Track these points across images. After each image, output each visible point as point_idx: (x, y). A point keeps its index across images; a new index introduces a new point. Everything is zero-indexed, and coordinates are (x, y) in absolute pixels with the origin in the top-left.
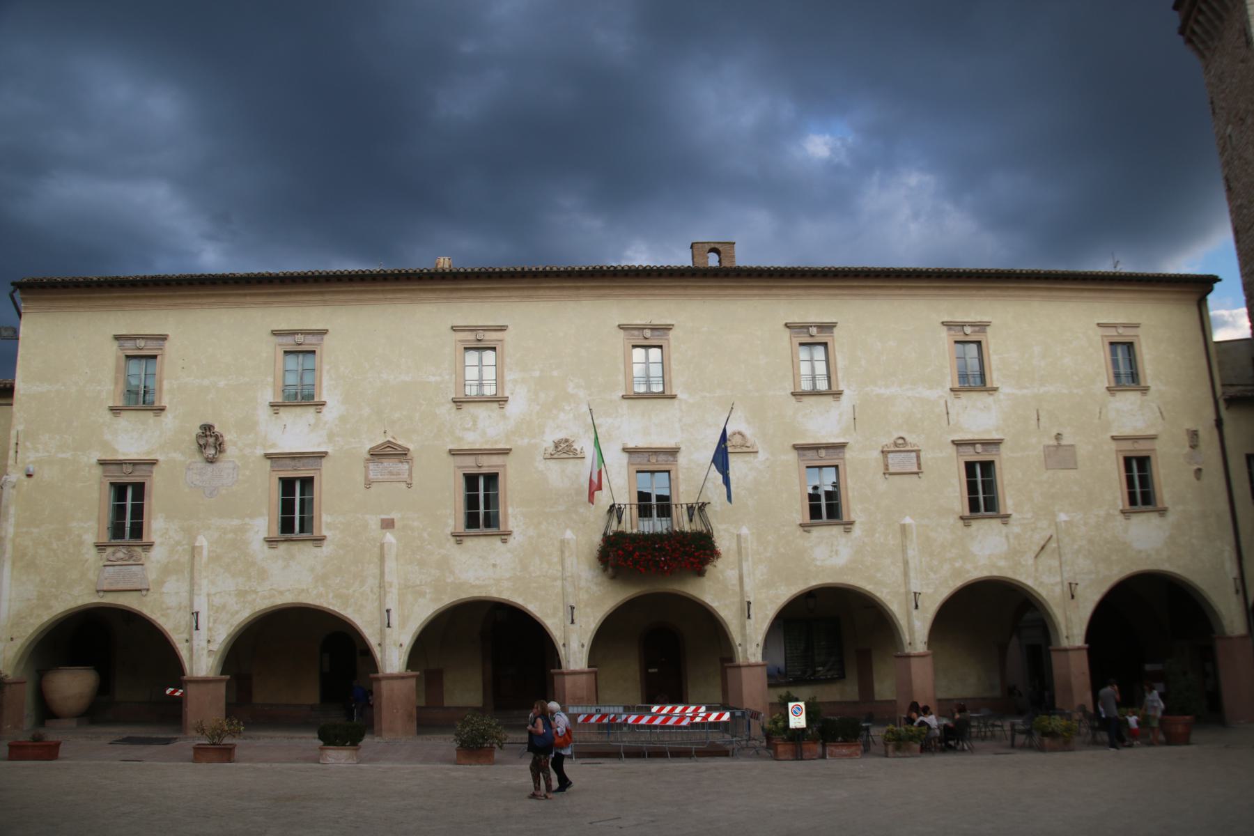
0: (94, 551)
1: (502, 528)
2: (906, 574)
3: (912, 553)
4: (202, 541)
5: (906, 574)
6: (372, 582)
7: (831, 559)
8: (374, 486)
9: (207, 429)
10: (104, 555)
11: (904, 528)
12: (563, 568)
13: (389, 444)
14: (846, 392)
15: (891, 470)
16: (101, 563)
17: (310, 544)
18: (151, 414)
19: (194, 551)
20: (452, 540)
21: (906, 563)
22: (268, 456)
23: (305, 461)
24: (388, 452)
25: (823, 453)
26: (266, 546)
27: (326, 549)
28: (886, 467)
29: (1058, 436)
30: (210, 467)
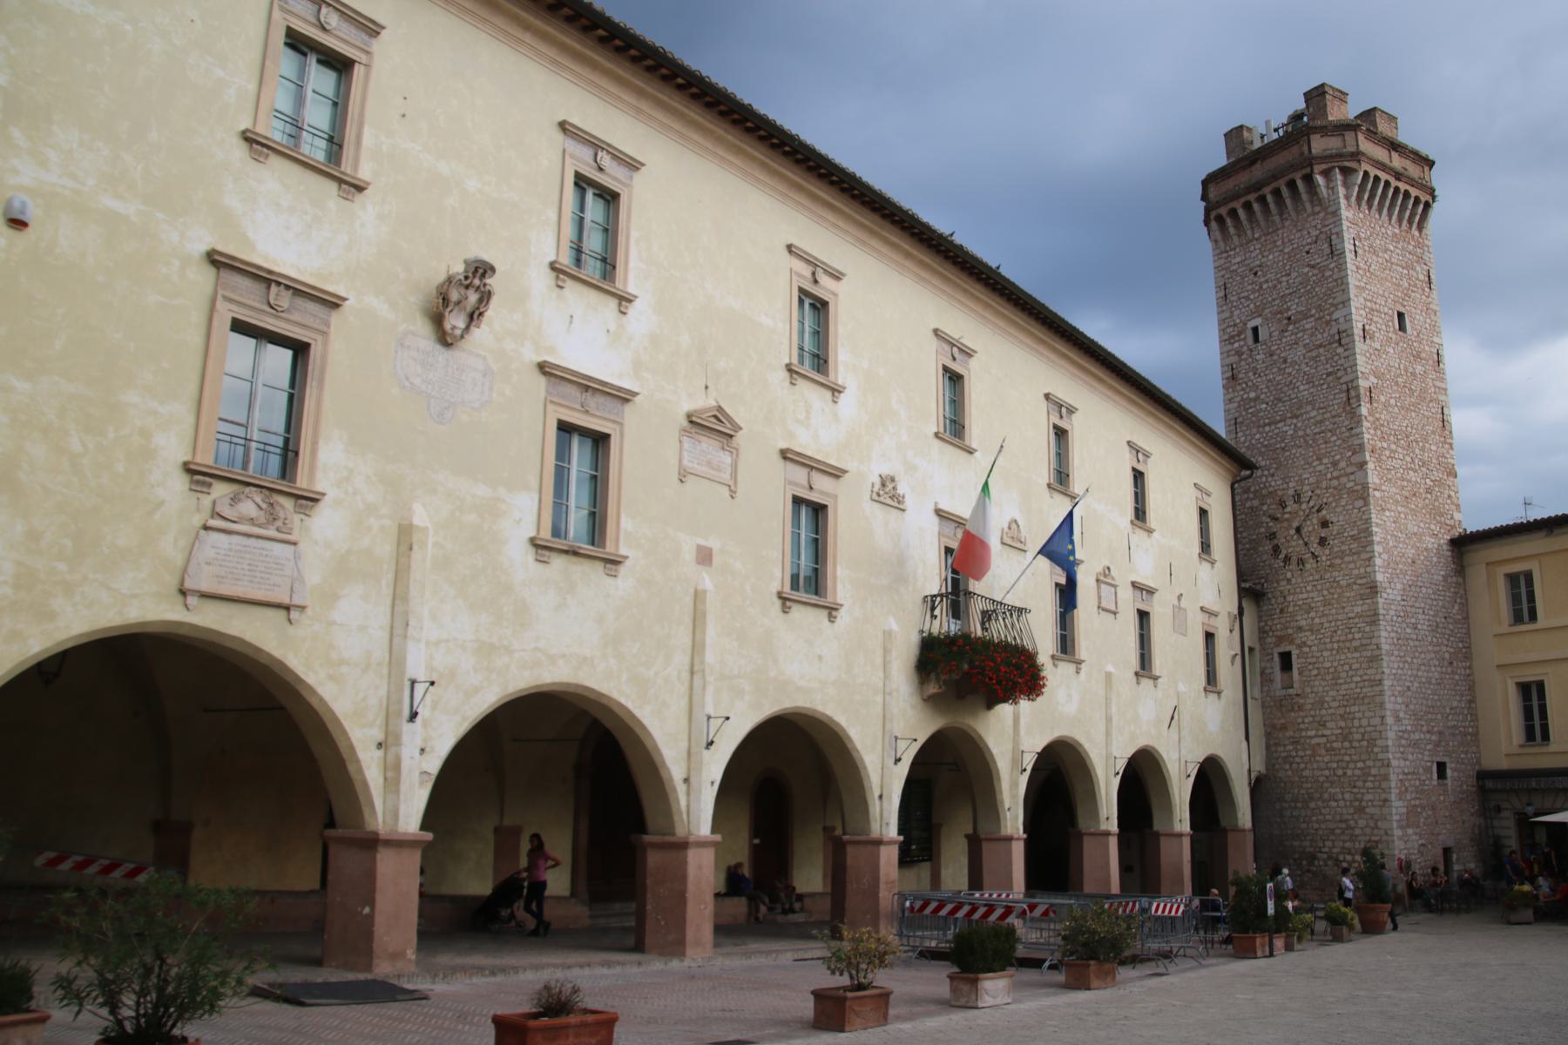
0: (180, 482)
1: (830, 598)
2: (1108, 733)
3: (1114, 709)
4: (420, 517)
5: (1108, 733)
6: (681, 660)
8: (690, 479)
9: (481, 270)
10: (207, 501)
11: (1108, 676)
12: (886, 677)
13: (720, 414)
15: (1104, 605)
16: (197, 520)
17: (599, 566)
18: (332, 187)
19: (405, 537)
20: (778, 603)
21: (1109, 720)
22: (544, 368)
23: (601, 399)
24: (713, 426)
26: (530, 554)
27: (624, 583)
29: (1180, 597)
30: (441, 354)
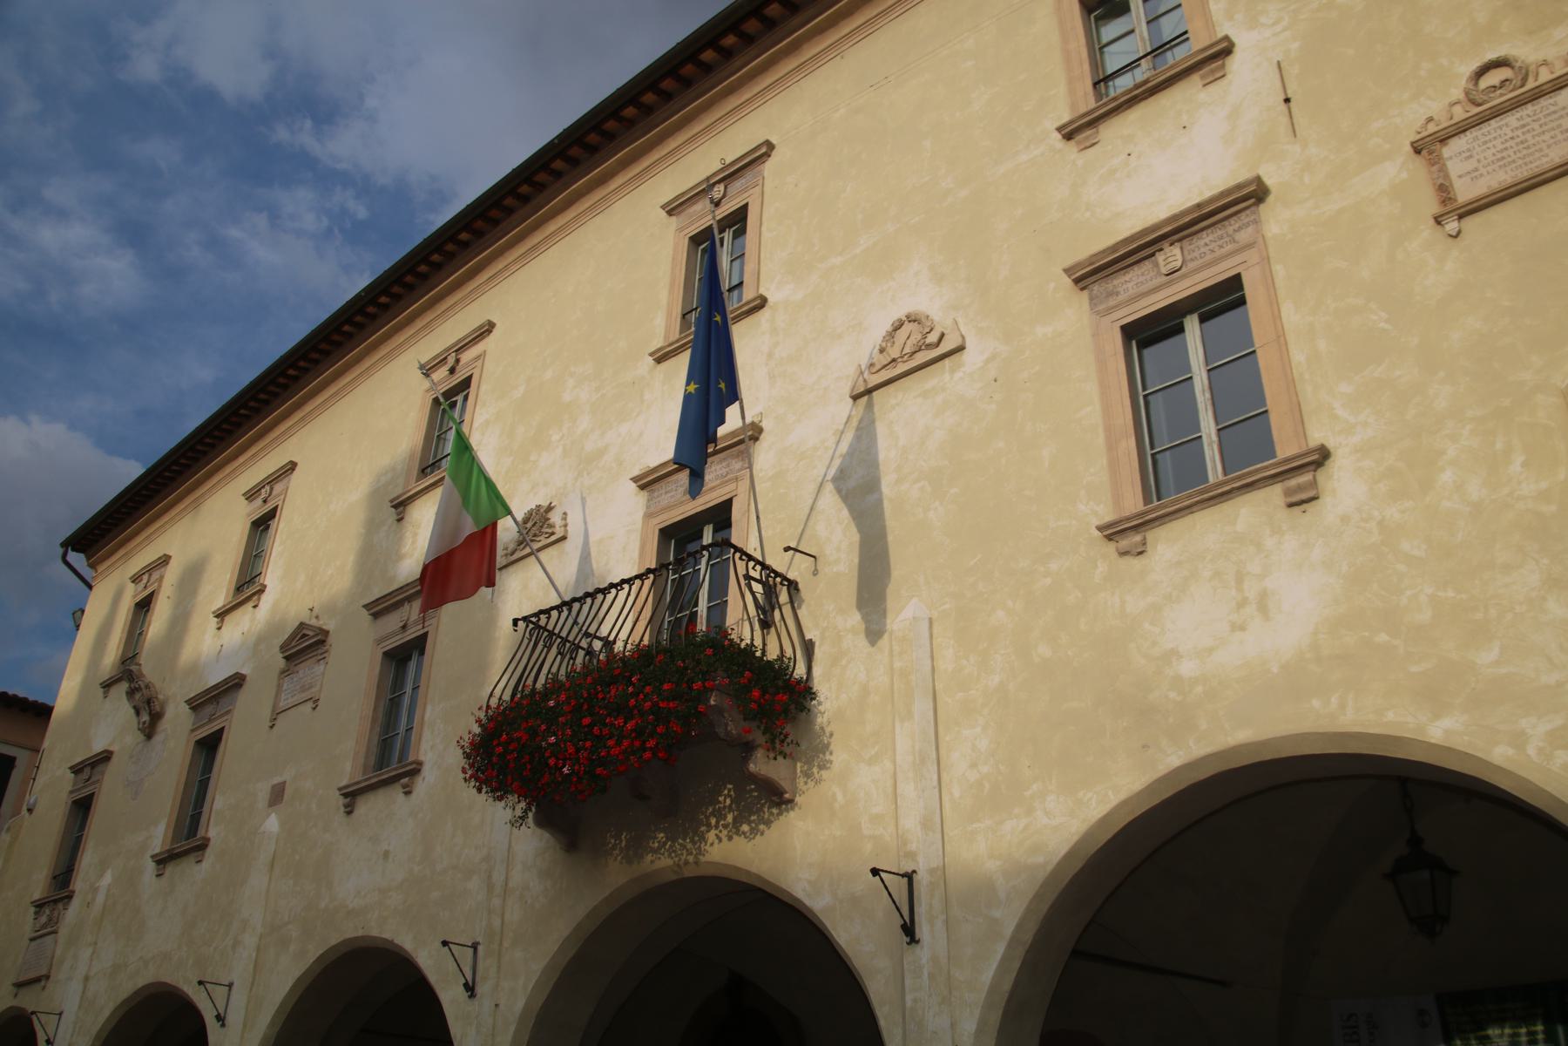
7: (1259, 640)
14: (1242, 40)
15: (1465, 192)
25: (1171, 256)
28: (1444, 191)
